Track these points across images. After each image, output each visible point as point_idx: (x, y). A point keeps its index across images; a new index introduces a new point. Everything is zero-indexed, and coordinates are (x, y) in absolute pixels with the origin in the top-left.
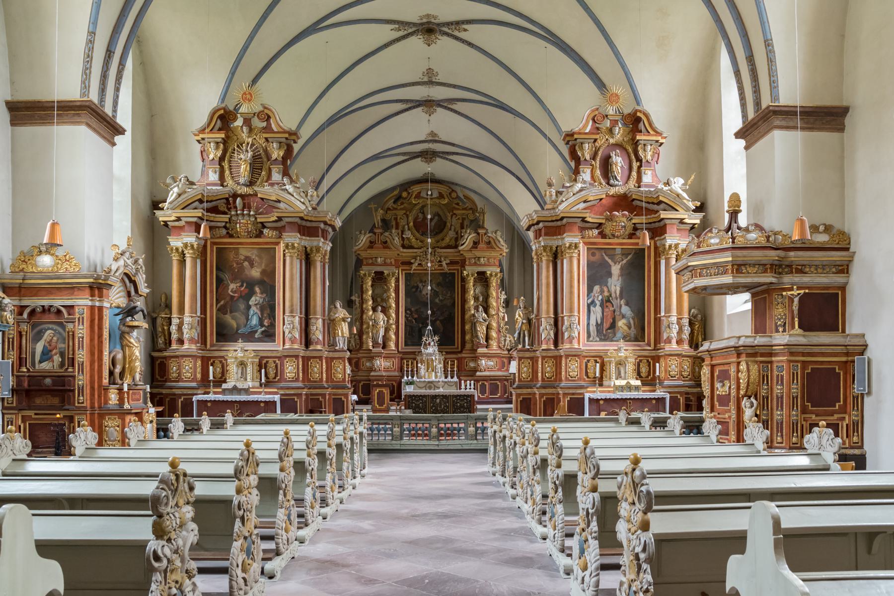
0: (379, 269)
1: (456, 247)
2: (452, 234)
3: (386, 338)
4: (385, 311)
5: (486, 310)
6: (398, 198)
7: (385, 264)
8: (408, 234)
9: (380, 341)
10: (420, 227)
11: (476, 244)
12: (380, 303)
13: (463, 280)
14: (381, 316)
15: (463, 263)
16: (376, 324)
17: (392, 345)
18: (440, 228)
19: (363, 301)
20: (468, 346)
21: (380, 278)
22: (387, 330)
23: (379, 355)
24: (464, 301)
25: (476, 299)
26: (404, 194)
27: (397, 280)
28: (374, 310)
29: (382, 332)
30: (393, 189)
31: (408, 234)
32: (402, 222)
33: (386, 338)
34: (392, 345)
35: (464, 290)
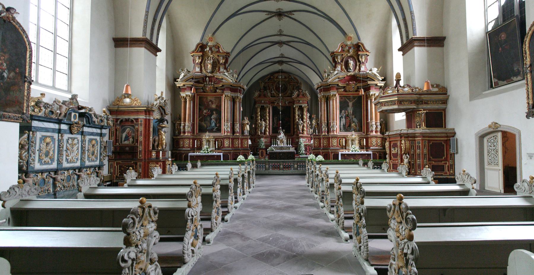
0: (262, 105)
1: (291, 96)
2: (289, 92)
3: (265, 131)
4: (265, 121)
5: (302, 120)
6: (270, 79)
7: (265, 103)
8: (273, 92)
9: (263, 131)
10: (277, 89)
11: (298, 95)
12: (263, 118)
13: (294, 109)
14: (264, 122)
15: (293, 103)
16: (261, 125)
17: (268, 133)
18: (285, 90)
19: (257, 117)
20: (295, 133)
21: (263, 109)
22: (265, 128)
23: (263, 137)
24: (294, 117)
25: (299, 116)
26: (272, 77)
27: (269, 109)
28: (261, 120)
29: (264, 128)
30: (268, 75)
31: (273, 92)
32: (271, 88)
33: (265, 131)
34: (268, 133)
35: (294, 113)
